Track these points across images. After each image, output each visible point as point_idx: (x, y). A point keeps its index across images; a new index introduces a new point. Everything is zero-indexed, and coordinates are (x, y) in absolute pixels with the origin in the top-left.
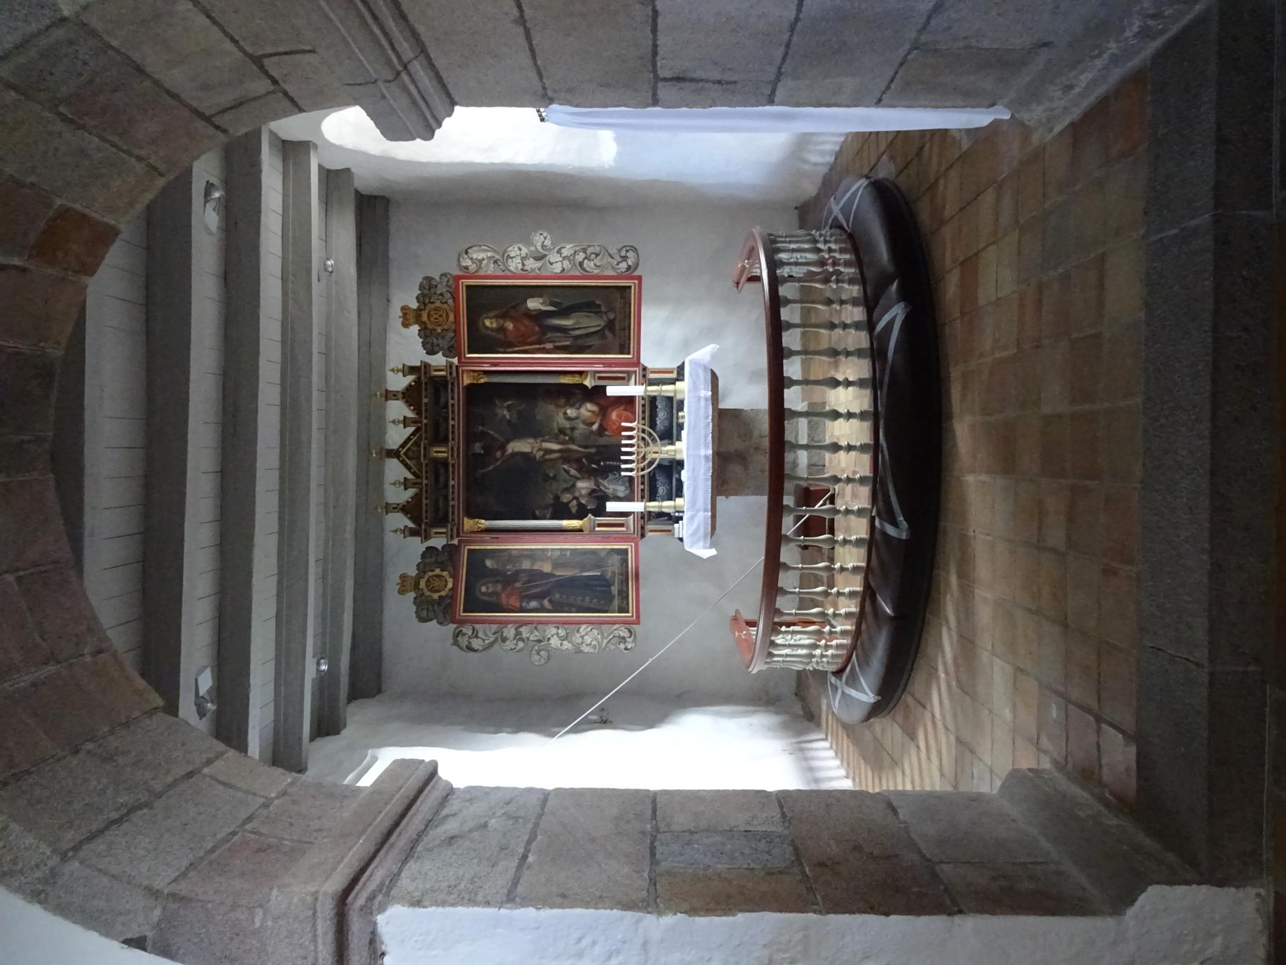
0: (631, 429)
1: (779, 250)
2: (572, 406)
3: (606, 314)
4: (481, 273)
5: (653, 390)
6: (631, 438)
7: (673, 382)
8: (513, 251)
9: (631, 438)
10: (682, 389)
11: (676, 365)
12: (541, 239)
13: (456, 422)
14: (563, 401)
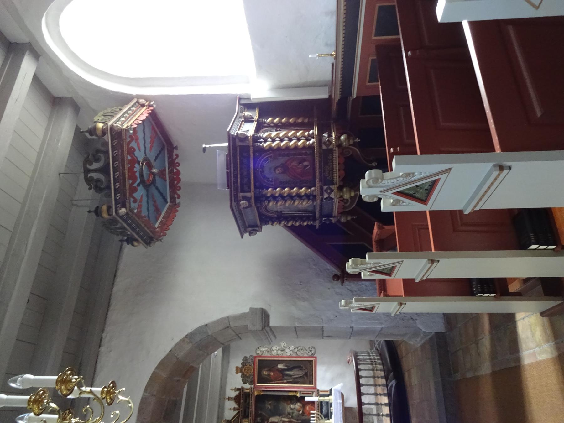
0: (314, 414)
1: (358, 356)
2: (293, 404)
3: (305, 370)
4: (263, 355)
5: (321, 399)
6: (314, 417)
7: (328, 396)
8: (274, 348)
9: (314, 417)
10: (332, 399)
11: (329, 389)
12: (283, 344)
13: (252, 409)
14: (289, 402)
